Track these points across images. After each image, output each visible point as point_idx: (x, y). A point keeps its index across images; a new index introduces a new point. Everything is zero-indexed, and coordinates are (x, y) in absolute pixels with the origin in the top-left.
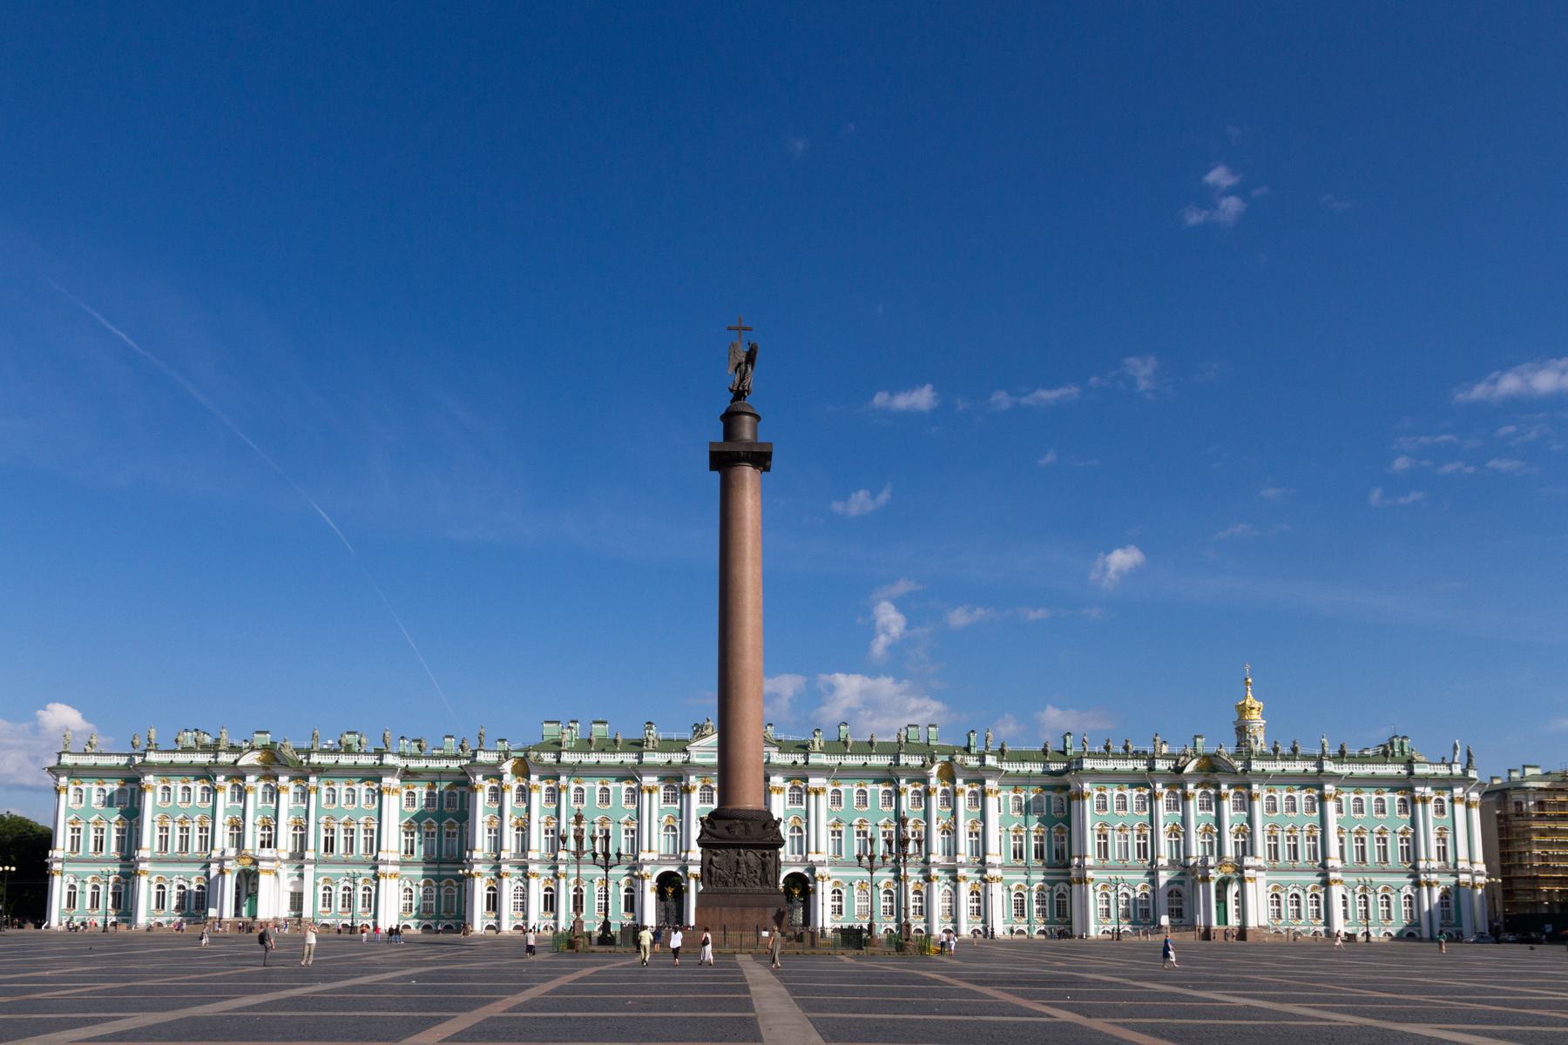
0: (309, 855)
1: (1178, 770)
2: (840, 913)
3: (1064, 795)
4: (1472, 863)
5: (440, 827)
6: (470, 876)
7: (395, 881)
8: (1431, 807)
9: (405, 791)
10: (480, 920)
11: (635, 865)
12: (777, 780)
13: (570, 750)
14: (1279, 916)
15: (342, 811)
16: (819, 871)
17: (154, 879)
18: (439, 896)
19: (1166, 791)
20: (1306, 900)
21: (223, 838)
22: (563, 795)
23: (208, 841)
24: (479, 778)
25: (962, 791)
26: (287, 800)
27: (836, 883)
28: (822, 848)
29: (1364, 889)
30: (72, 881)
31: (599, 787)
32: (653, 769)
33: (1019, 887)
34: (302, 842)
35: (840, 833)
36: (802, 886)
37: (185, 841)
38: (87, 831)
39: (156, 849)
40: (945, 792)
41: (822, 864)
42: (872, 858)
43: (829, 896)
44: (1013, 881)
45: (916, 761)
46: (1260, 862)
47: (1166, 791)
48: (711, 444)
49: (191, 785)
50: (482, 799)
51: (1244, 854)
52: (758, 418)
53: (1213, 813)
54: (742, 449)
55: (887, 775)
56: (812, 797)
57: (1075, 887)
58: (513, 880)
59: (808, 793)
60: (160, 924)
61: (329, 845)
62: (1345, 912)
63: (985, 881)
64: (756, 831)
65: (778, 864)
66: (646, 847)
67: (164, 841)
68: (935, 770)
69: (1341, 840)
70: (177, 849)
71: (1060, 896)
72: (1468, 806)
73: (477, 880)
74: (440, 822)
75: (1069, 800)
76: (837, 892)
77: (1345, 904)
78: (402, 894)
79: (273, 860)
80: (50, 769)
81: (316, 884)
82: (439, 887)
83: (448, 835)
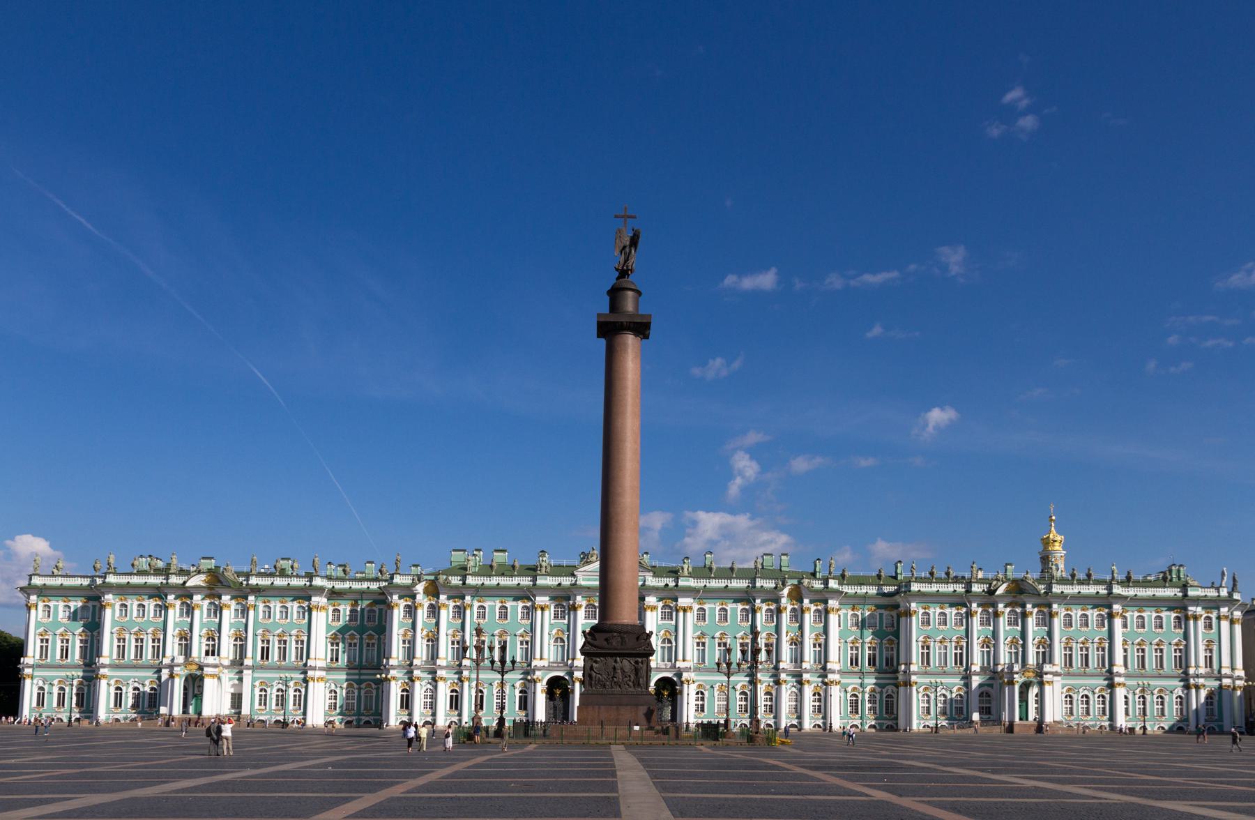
1: (991, 592)
2: (703, 710)
3: (894, 613)
4: (1233, 669)
5: (361, 639)
6: (387, 679)
7: (322, 684)
8: (1201, 623)
9: (331, 609)
10: (394, 718)
11: (528, 671)
12: (651, 600)
13: (474, 574)
14: (1072, 713)
15: (275, 624)
16: (685, 675)
17: (112, 682)
18: (359, 696)
19: (980, 610)
20: (1094, 700)
21: (173, 648)
22: (468, 612)
23: (159, 650)
24: (395, 597)
25: (809, 609)
26: (228, 616)
27: (700, 686)
28: (689, 657)
29: (1143, 690)
30: (41, 684)
31: (498, 605)
32: (545, 590)
33: (854, 689)
34: (241, 651)
35: (704, 644)
36: (671, 689)
37: (139, 651)
38: (54, 643)
39: (115, 656)
40: (793, 610)
41: (688, 670)
42: (729, 665)
43: (693, 696)
44: (849, 684)
45: (770, 584)
46: (1057, 669)
47: (980, 610)
48: (599, 315)
49: (146, 603)
50: (398, 615)
51: (1044, 661)
52: (639, 293)
53: (1019, 628)
54: (624, 320)
55: (744, 596)
56: (681, 614)
57: (901, 689)
58: (424, 683)
59: (677, 611)
60: (117, 720)
61: (265, 653)
62: (1127, 710)
63: (826, 684)
64: (630, 642)
65: (649, 669)
66: (538, 656)
67: (122, 651)
68: (786, 592)
69: (1125, 651)
70: (132, 657)
71: (888, 696)
72: (1232, 622)
73: (393, 683)
74: (361, 635)
75: (899, 616)
76: (700, 694)
77: (1126, 703)
78: (328, 695)
79: (216, 666)
80: (22, 589)
81: (253, 687)
82: (360, 689)
83: (368, 645)
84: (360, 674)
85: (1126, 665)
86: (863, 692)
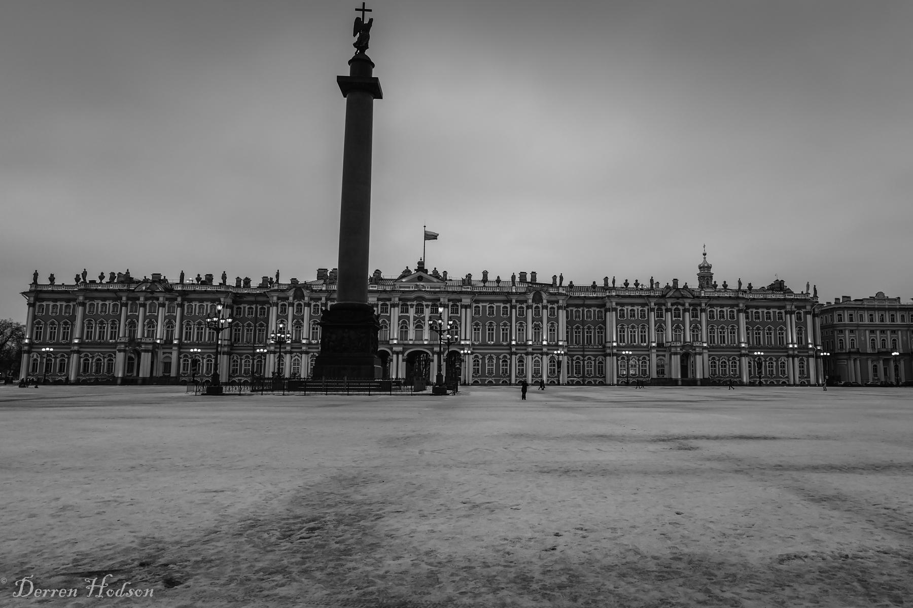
3: (603, 310)
4: (816, 345)
18: (253, 364)
19: (656, 307)
24: (275, 298)
27: (476, 357)
33: (578, 358)
37: (101, 335)
56: (464, 310)
62: (750, 371)
68: (531, 296)
72: (814, 316)
76: (476, 363)
77: (750, 367)
80: (23, 293)
81: (179, 358)
82: (253, 360)
85: (748, 342)
86: (584, 361)
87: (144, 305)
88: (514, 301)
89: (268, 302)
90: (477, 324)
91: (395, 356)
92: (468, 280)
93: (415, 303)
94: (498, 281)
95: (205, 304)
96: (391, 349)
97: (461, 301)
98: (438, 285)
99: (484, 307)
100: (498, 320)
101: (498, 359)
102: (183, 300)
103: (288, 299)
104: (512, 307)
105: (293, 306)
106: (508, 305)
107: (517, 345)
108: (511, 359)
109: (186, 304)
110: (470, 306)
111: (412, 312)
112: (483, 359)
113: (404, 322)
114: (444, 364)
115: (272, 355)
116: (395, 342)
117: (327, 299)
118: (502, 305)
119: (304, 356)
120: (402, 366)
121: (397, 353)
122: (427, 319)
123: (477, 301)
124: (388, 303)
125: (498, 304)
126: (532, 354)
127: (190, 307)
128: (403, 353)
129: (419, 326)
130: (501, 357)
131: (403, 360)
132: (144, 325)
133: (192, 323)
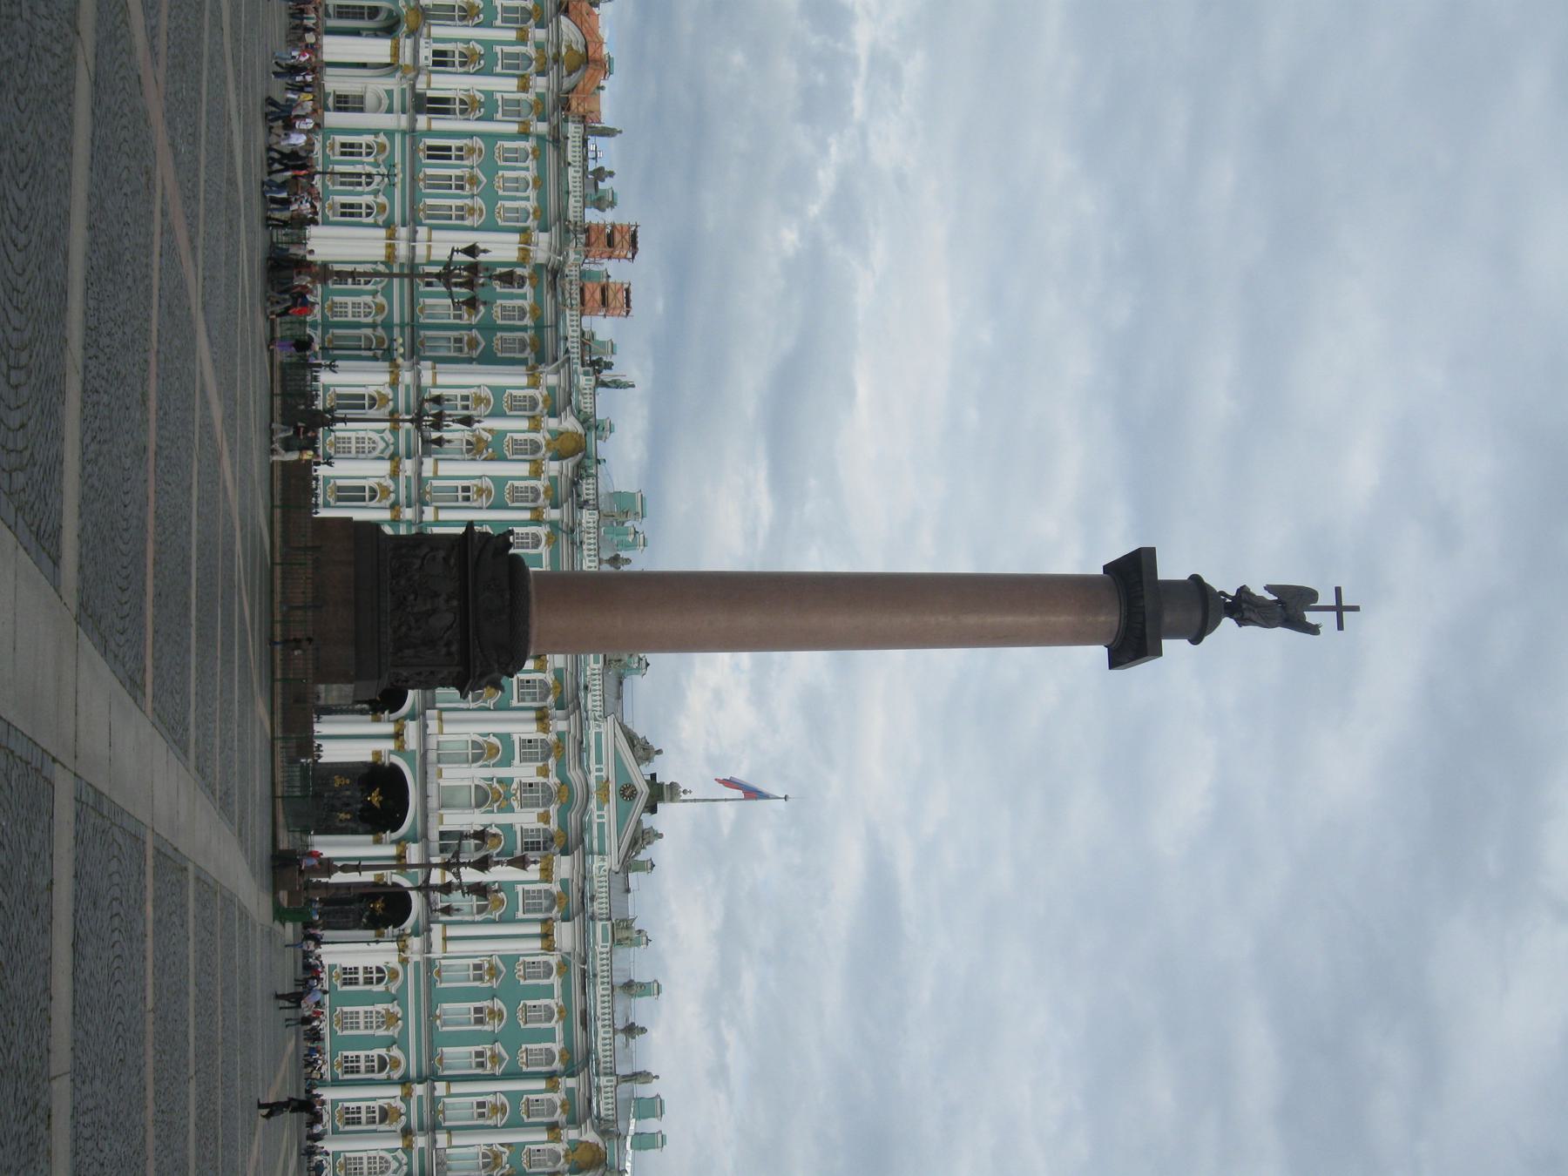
0: (422, 121)
5: (470, 327)
7: (379, 252)
12: (564, 866)
15: (491, 169)
16: (415, 943)
18: (358, 325)
24: (552, 380)
26: (505, 86)
27: (394, 974)
34: (439, 106)
41: (428, 946)
56: (537, 929)
58: (388, 436)
68: (591, 1136)
74: (477, 327)
81: (376, 132)
82: (374, 326)
83: (459, 340)
84: (402, 326)
87: (522, 40)
88: (571, 1082)
89: (541, 359)
90: (493, 971)
91: (390, 728)
92: (625, 933)
93: (553, 780)
94: (631, 1030)
95: (531, 193)
96: (412, 716)
97: (565, 919)
98: (612, 843)
99: (548, 992)
100: (513, 1037)
101: (390, 1042)
102: (540, 138)
103: (554, 413)
104: (551, 1076)
105: (536, 429)
106: (557, 1065)
107: (434, 1100)
108: (388, 1082)
109: (528, 145)
110: (549, 948)
111: (523, 772)
112: (393, 999)
113: (493, 750)
114: (368, 877)
115: (386, 378)
116: (433, 726)
117: (554, 525)
118: (556, 1047)
119: (385, 467)
120: (361, 753)
121: (398, 736)
122: (504, 818)
123: (564, 966)
124: (551, 699)
125: (559, 1035)
126: (407, 1149)
127: (518, 157)
128: (400, 750)
129: (483, 798)
130: (395, 1052)
131: (377, 754)
132: (467, 41)
133: (474, 160)
